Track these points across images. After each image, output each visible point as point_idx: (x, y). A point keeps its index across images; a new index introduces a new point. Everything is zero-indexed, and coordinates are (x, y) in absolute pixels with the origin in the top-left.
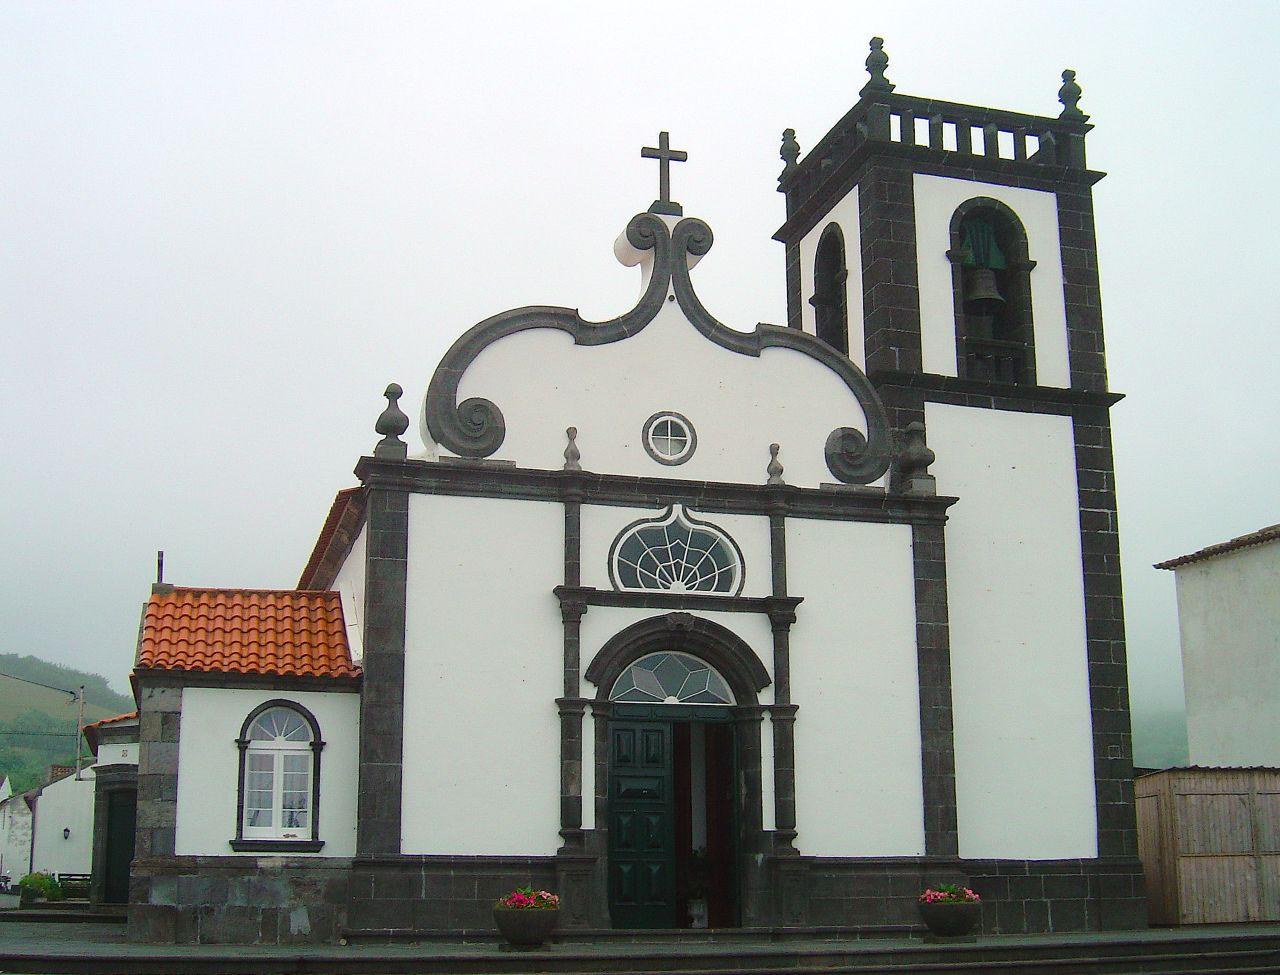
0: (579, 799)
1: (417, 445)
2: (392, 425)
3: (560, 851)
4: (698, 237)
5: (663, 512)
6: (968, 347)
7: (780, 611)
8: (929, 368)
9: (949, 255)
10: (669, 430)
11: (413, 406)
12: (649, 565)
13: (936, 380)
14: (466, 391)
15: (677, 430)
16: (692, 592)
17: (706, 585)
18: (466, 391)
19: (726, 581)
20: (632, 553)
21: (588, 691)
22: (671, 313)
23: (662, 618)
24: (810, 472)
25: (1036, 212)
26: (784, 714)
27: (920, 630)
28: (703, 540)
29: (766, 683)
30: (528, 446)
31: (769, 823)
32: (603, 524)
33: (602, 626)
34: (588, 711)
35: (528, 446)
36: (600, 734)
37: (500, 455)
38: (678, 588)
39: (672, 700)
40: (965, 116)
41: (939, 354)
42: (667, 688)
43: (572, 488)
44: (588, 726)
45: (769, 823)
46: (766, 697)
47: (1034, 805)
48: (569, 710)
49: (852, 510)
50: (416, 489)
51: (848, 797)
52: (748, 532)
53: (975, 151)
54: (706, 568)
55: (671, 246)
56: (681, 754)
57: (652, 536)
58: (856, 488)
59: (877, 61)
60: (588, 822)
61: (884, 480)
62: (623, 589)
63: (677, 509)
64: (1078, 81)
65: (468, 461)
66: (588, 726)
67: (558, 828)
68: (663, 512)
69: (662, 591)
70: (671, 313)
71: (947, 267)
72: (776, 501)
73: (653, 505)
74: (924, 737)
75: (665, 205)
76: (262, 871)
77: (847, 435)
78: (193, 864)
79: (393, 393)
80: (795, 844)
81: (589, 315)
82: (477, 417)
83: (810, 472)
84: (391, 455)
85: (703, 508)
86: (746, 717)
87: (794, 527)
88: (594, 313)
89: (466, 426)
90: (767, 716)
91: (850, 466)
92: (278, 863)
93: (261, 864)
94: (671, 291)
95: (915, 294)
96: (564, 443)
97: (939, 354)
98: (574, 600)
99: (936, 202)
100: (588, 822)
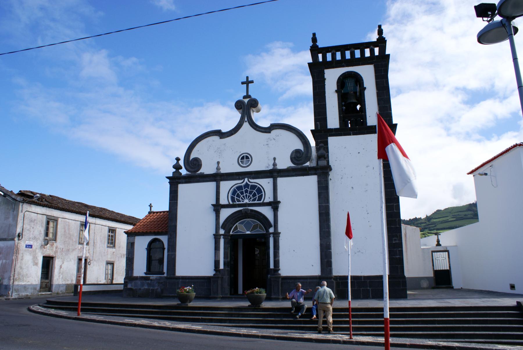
0: (219, 261)
1: (184, 172)
2: (177, 167)
3: (214, 275)
4: (253, 103)
5: (242, 181)
6: (343, 119)
7: (275, 205)
8: (329, 126)
9: (336, 91)
10: (245, 158)
11: (181, 163)
12: (238, 196)
13: (331, 130)
14: (192, 156)
15: (247, 158)
16: (251, 202)
17: (254, 200)
18: (192, 156)
19: (260, 198)
20: (236, 192)
21: (222, 232)
22: (246, 125)
23: (241, 210)
24: (285, 163)
25: (367, 73)
26: (276, 235)
27: (320, 207)
28: (253, 187)
29: (271, 226)
30: (207, 169)
31: (272, 266)
32: (226, 186)
33: (225, 213)
34: (222, 237)
35: (207, 169)
36: (225, 243)
37: (201, 171)
38: (246, 201)
39: (248, 232)
40: (342, 48)
41: (333, 120)
42: (243, 228)
43: (218, 177)
44: (222, 241)
45: (272, 266)
46: (271, 230)
47: (362, 255)
48: (217, 237)
49: (294, 174)
50: (180, 183)
51: (296, 256)
52: (266, 184)
53: (347, 58)
54: (254, 195)
55: (245, 107)
56: (248, 247)
57: (240, 188)
58: (299, 166)
59: (314, 40)
60: (222, 267)
61: (312, 163)
62: (231, 203)
63: (246, 180)
64: (382, 27)
65: (193, 174)
66: (222, 241)
67: (214, 268)
68: (242, 181)
69: (242, 203)
70: (246, 125)
71: (336, 95)
72: (274, 174)
73: (239, 179)
74: (321, 239)
75: (247, 96)
76: (151, 280)
77: (297, 151)
78: (137, 278)
79: (178, 159)
80: (279, 272)
81: (224, 130)
82: (195, 162)
83: (285, 163)
84: (177, 175)
85: (254, 178)
86: (266, 237)
87: (280, 180)
88: (225, 129)
89: (194, 164)
90: (272, 236)
91: (297, 160)
92: (154, 278)
93: (151, 278)
94: (246, 119)
95: (325, 105)
96: (216, 166)
97: (333, 120)
98: (217, 207)
99: (332, 76)
100: (222, 267)
